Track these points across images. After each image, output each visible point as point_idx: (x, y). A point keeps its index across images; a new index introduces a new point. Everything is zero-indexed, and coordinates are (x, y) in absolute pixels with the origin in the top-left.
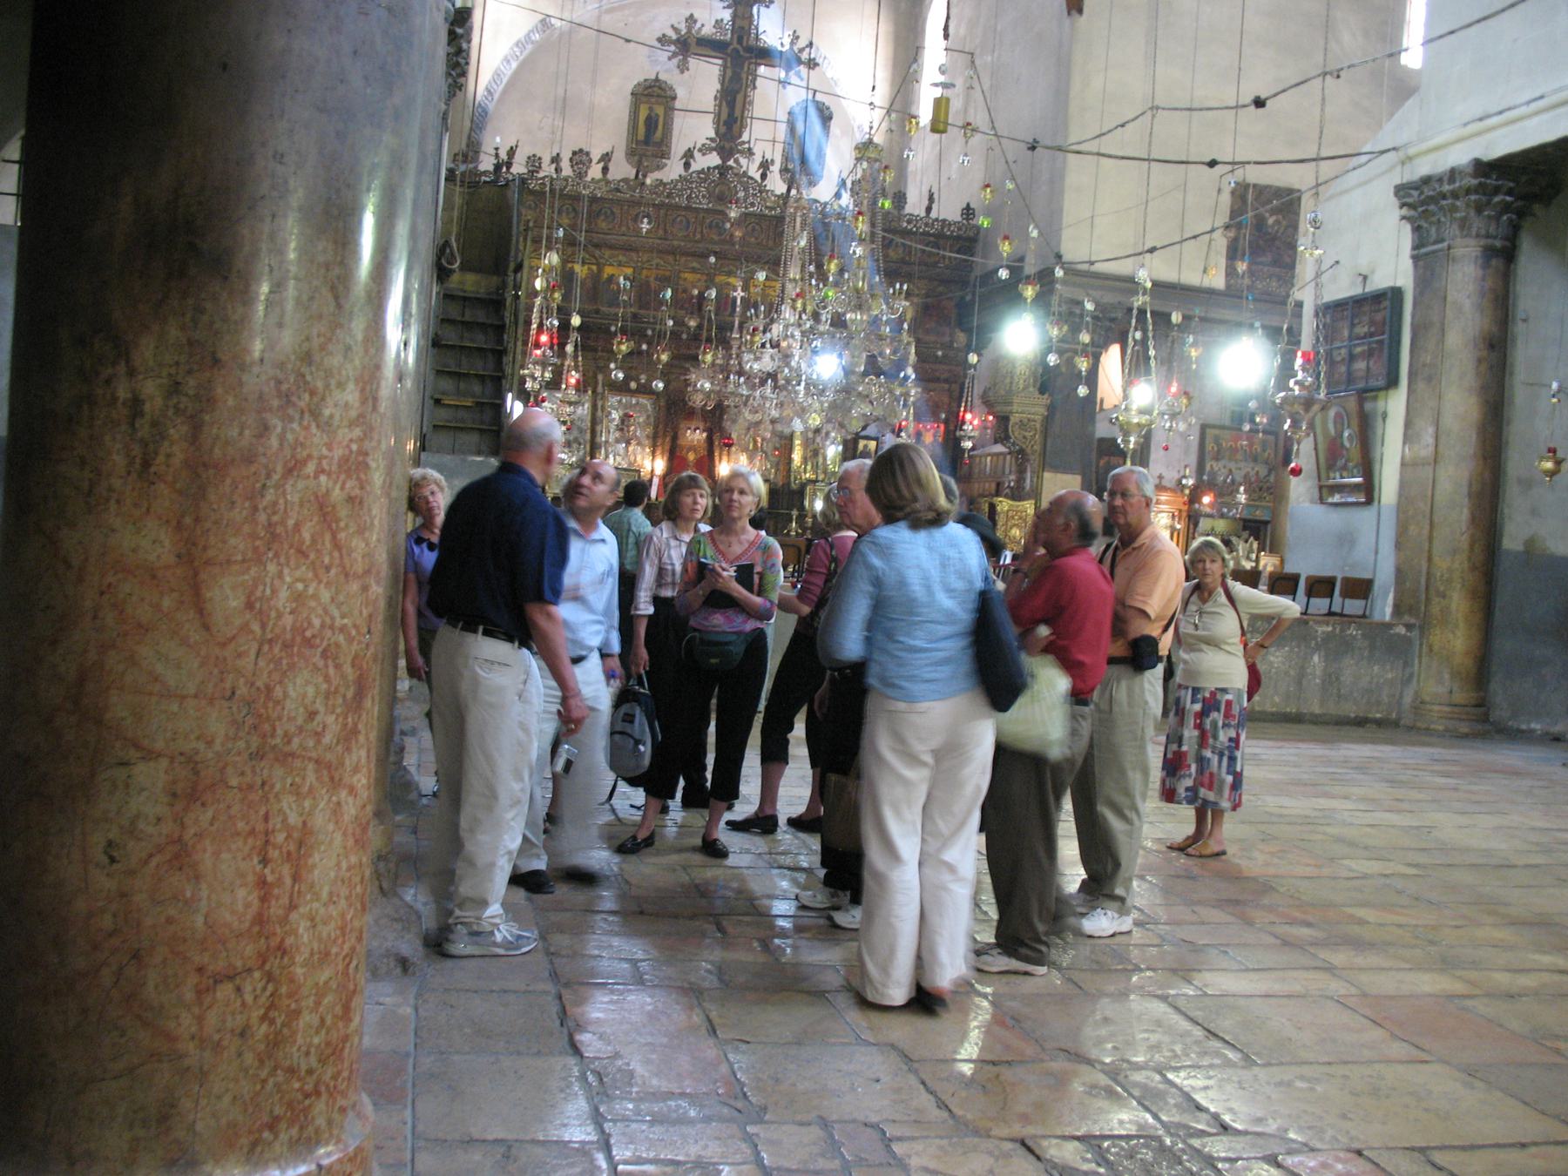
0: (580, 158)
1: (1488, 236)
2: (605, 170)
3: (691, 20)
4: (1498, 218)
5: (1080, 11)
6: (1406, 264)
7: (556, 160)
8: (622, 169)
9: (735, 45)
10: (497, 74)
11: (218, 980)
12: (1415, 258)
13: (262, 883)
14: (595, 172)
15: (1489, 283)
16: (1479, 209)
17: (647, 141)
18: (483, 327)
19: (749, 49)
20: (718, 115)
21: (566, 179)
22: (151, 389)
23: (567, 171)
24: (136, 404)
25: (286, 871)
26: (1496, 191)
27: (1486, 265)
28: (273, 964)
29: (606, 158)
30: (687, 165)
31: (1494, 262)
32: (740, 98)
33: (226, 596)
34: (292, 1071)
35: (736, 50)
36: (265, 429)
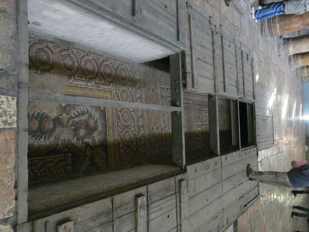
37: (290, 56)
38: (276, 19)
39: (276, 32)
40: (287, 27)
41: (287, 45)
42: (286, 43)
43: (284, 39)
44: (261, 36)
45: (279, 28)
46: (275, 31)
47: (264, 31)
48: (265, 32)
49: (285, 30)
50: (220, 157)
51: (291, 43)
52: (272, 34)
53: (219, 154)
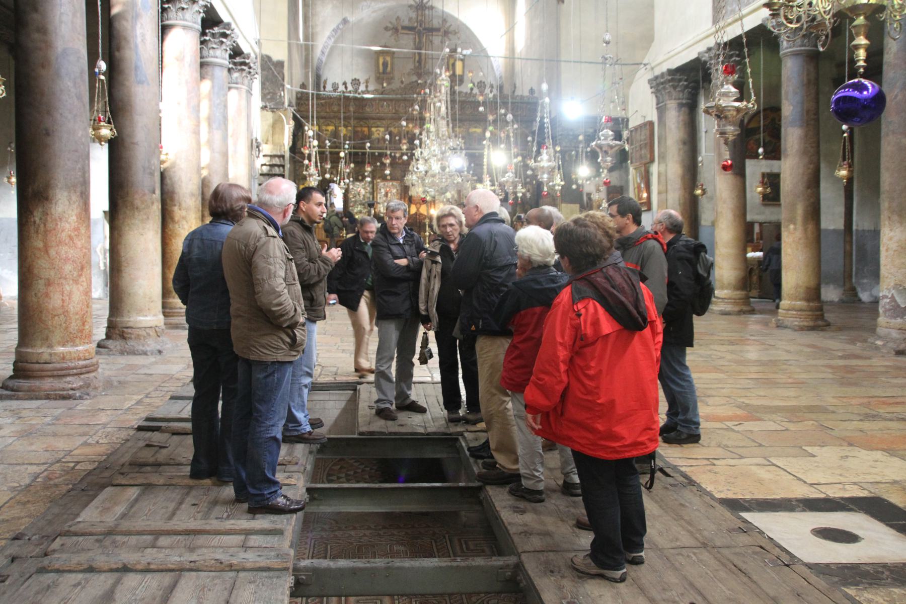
1: (679, 99)
6: (655, 112)
7: (345, 84)
9: (419, 27)
11: (55, 316)
12: (657, 109)
13: (63, 300)
15: (681, 118)
16: (675, 87)
17: (384, 72)
18: (279, 166)
22: (37, 219)
23: (350, 88)
24: (35, 222)
25: (67, 298)
27: (679, 111)
28: (66, 314)
31: (683, 109)
33: (52, 252)
34: (71, 333)
36: (57, 224)
37: (165, 324)
38: (40, 354)
39: (81, 355)
40: (73, 324)
41: (129, 330)
42: (123, 332)
43: (108, 336)
44: (86, 402)
45: (72, 346)
46: (79, 359)
47: (71, 392)
48: (72, 389)
49: (82, 331)
50: (524, 557)
51: (126, 319)
52: (86, 367)
53: (512, 560)
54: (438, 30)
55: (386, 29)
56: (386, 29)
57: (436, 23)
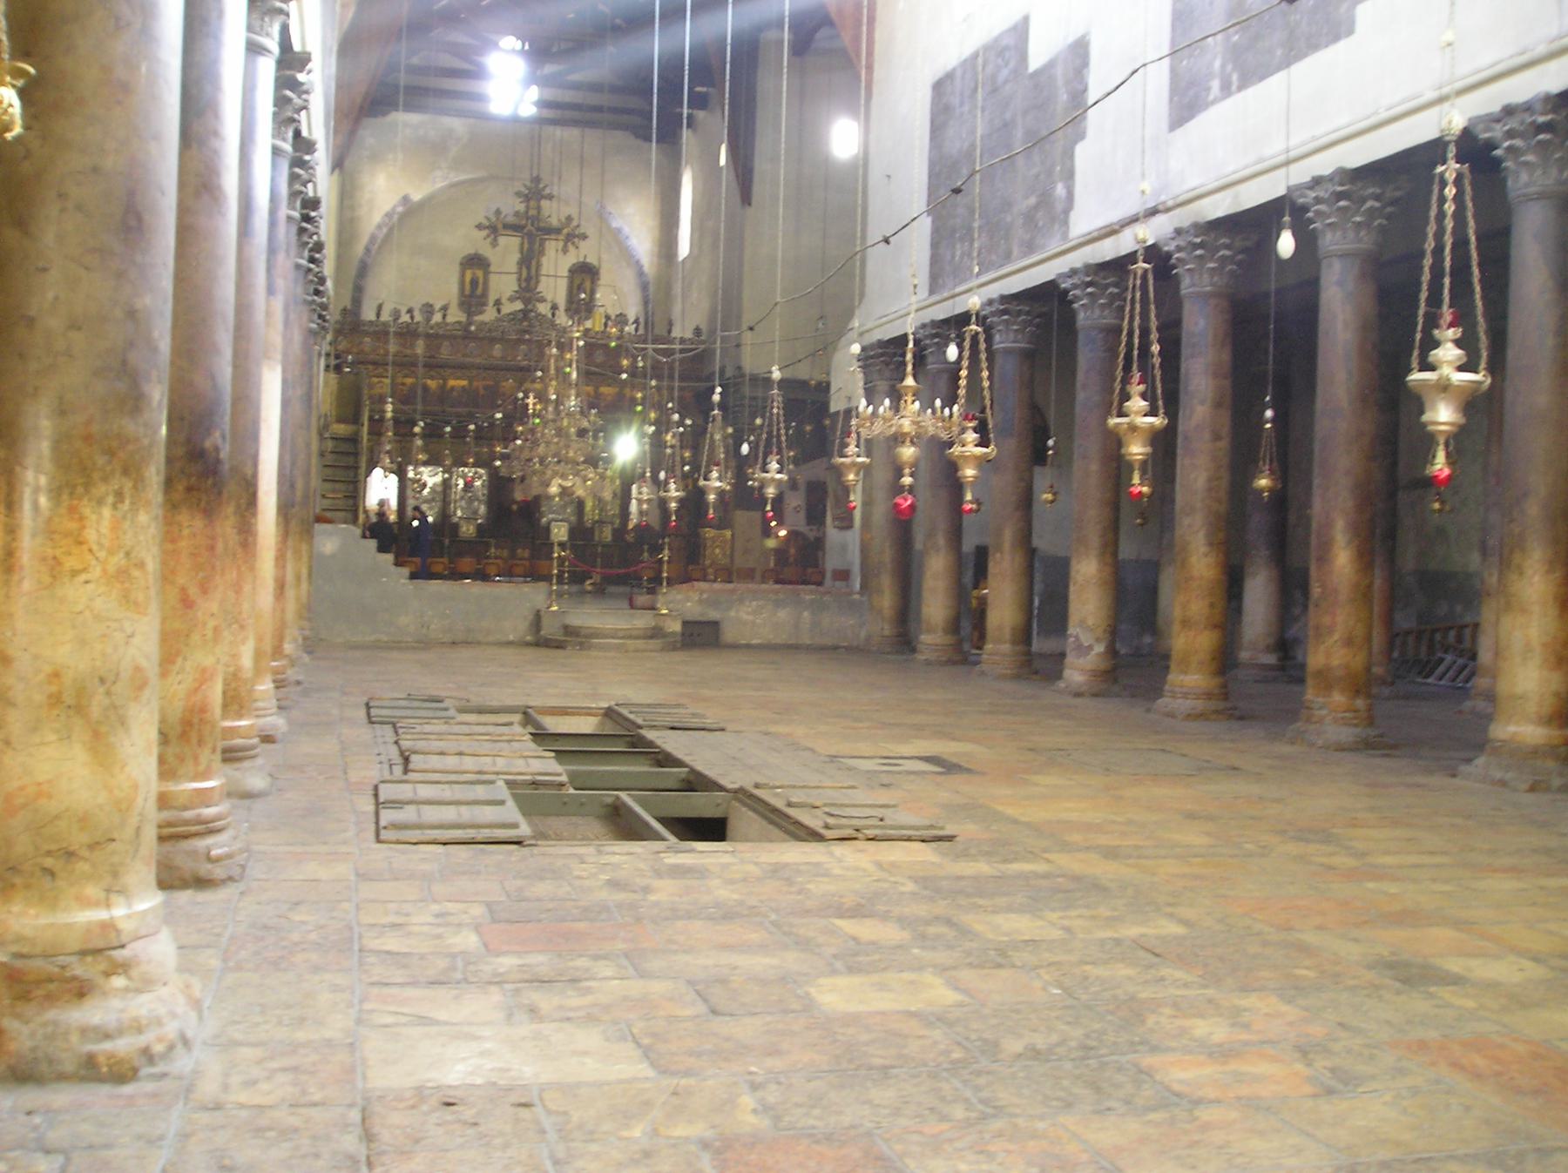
0: (428, 309)
2: (444, 317)
3: (498, 212)
4: (1021, 331)
5: (750, 204)
8: (456, 316)
9: (529, 227)
10: (373, 238)
12: (865, 389)
14: (437, 318)
16: (887, 364)
18: (348, 454)
19: (539, 229)
20: (520, 273)
21: (418, 323)
23: (418, 317)
26: (1019, 313)
29: (445, 309)
30: (499, 311)
32: (534, 263)
35: (530, 231)
54: (558, 231)
55: (479, 227)
56: (479, 227)
57: (554, 222)
